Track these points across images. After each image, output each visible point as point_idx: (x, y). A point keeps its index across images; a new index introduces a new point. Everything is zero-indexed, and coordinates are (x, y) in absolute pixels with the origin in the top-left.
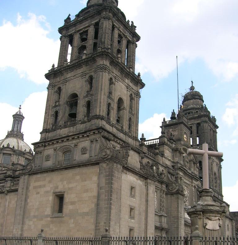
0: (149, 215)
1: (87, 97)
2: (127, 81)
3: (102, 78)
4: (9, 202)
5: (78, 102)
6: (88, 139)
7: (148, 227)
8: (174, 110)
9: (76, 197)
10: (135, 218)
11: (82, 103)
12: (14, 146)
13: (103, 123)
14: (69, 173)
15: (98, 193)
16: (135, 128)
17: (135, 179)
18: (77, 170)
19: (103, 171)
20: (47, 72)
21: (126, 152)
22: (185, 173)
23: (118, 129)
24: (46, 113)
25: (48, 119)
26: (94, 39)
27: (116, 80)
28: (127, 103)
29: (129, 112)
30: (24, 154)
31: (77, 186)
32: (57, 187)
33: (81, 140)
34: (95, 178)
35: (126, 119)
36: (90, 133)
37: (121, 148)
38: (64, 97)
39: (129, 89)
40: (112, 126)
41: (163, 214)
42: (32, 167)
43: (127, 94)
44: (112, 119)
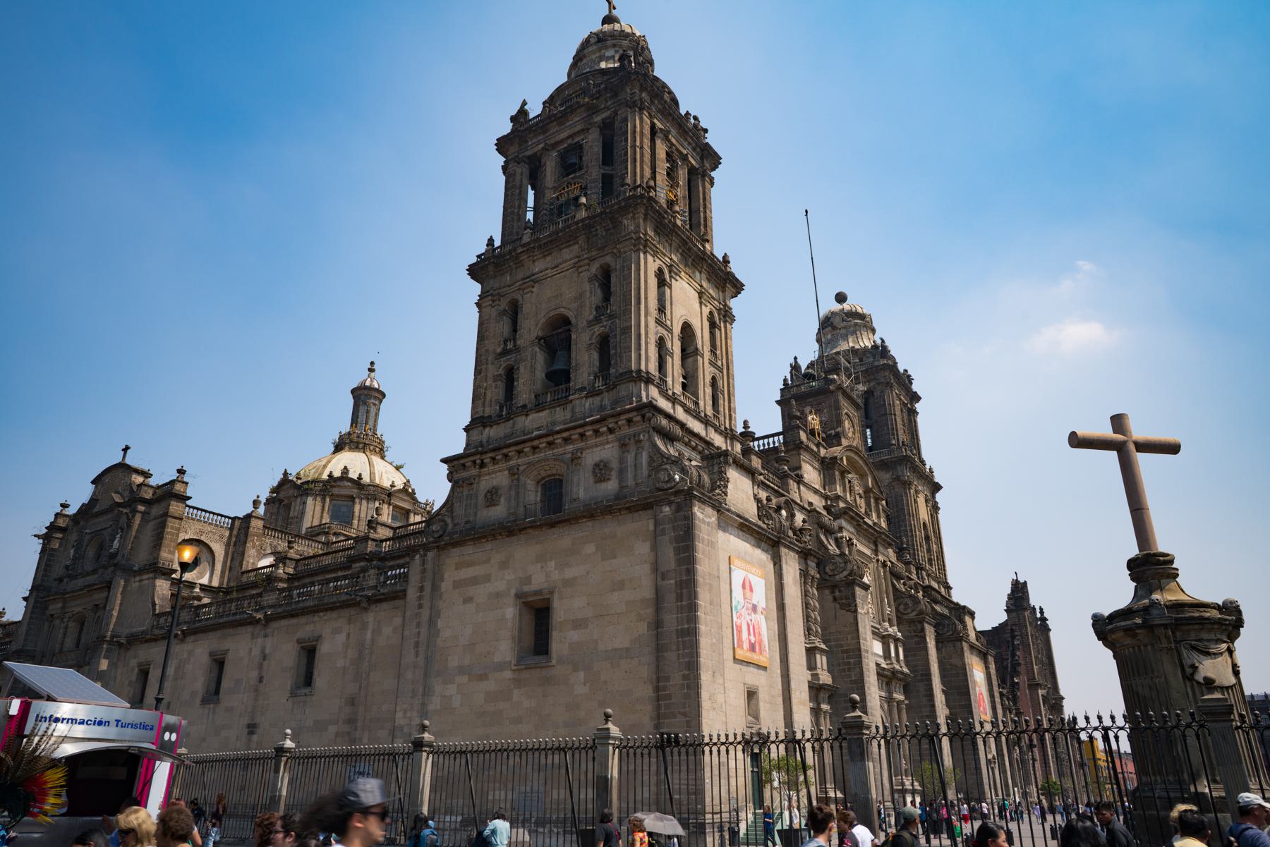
1: (598, 323)
4: (373, 632)
5: (574, 337)
6: (611, 437)
8: (796, 358)
12: (360, 475)
14: (563, 539)
15: (657, 590)
18: (587, 528)
19: (667, 526)
20: (474, 260)
23: (687, 411)
24: (478, 372)
25: (486, 389)
26: (603, 164)
27: (673, 274)
30: (390, 495)
31: (588, 573)
32: (528, 580)
33: (592, 442)
36: (617, 423)
41: (818, 645)
42: (446, 525)
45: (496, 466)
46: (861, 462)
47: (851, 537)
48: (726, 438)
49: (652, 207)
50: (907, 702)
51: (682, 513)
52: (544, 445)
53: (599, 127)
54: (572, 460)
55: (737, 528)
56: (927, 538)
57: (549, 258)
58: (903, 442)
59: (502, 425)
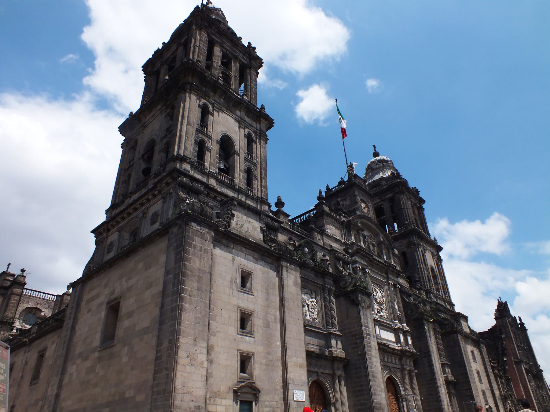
0: (289, 327)
2: (238, 113)
5: (155, 148)
7: (289, 352)
9: (135, 301)
10: (254, 334)
11: (158, 148)
13: (186, 167)
16: (259, 184)
22: (372, 262)
23: (221, 182)
27: (215, 108)
28: (240, 145)
29: (246, 160)
31: (138, 281)
33: (152, 202)
34: (163, 259)
36: (161, 186)
38: (141, 149)
39: (243, 124)
40: (209, 175)
44: (207, 164)
46: (373, 226)
47: (364, 267)
48: (257, 202)
50: (416, 371)
51: (181, 230)
56: (435, 277)
58: (412, 222)
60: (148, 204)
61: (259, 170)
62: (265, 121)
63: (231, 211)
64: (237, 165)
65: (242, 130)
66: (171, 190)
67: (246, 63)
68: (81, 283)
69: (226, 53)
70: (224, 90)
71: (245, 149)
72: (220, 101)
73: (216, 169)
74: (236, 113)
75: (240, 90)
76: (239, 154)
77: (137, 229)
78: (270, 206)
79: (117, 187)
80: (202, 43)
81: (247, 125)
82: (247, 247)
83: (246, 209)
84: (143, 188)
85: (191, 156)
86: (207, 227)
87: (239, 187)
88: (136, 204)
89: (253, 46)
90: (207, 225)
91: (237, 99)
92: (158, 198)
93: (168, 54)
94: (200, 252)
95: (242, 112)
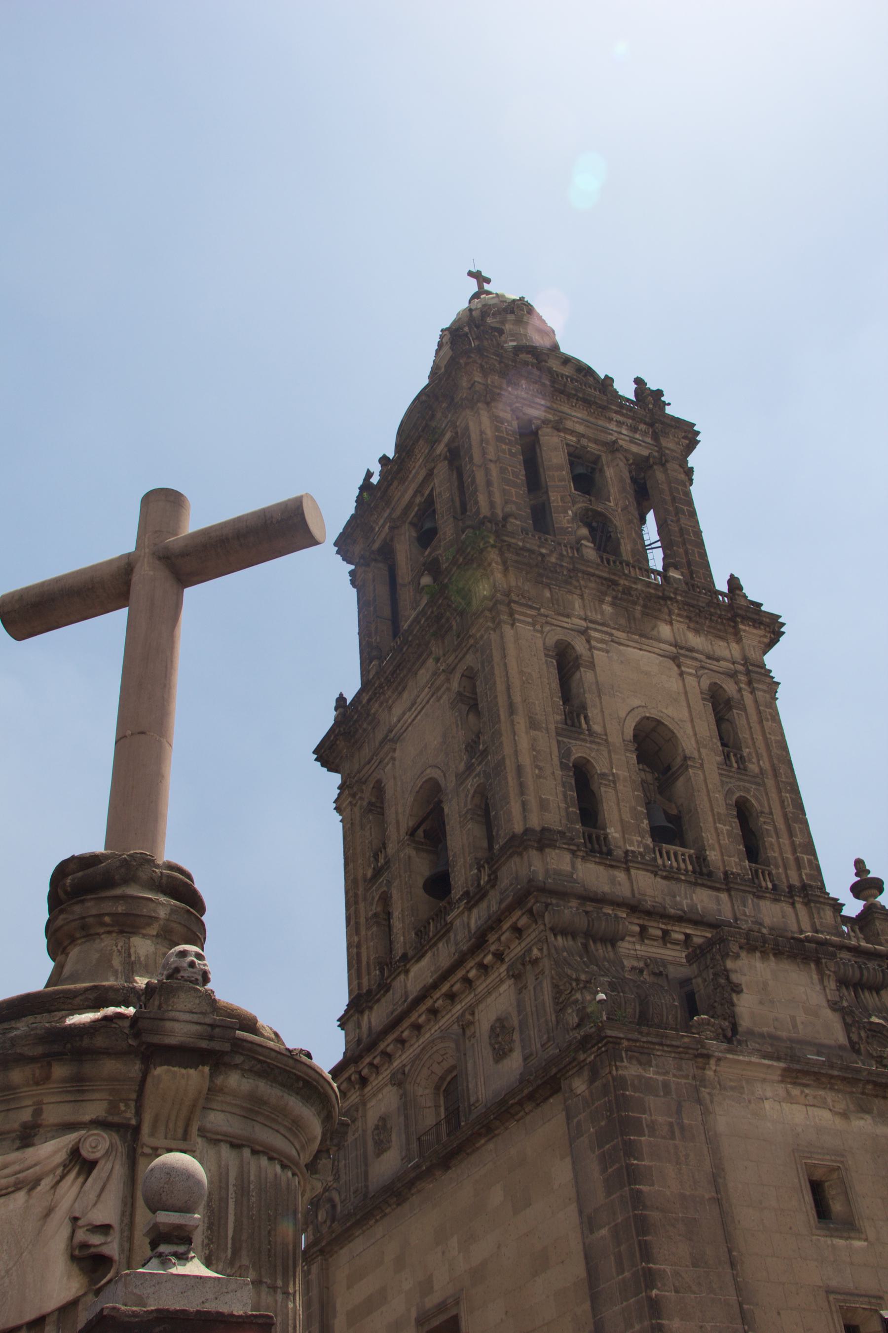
2: (665, 630)
3: (504, 656)
5: (446, 810)
6: (503, 968)
15: (586, 1257)
16: (785, 841)
17: (824, 1116)
19: (582, 1117)
21: (715, 975)
28: (695, 734)
33: (481, 987)
35: (712, 810)
36: (499, 939)
37: (691, 959)
39: (689, 662)
42: (334, 1206)
43: (686, 693)
44: (614, 833)
45: (380, 1078)
49: (509, 545)
51: (598, 1083)
52: (423, 1017)
53: (445, 458)
54: (463, 1029)
55: (782, 1081)
57: (405, 695)
59: (383, 1000)
60: (470, 993)
61: (774, 795)
62: (755, 627)
63: (728, 978)
64: (702, 803)
65: (691, 681)
66: (535, 952)
67: (645, 453)
68: (318, 1256)
69: (578, 446)
70: (606, 579)
71: (714, 740)
72: (602, 613)
73: (643, 838)
74: (659, 632)
75: (647, 543)
76: (702, 765)
77: (454, 1067)
78: (837, 906)
79: (356, 939)
80: (504, 447)
81: (701, 661)
82: (804, 1081)
83: (772, 957)
84: (440, 939)
85: (564, 821)
86: (673, 1055)
87: (726, 873)
88: (431, 997)
89: (652, 385)
90: (669, 1049)
91: (652, 591)
92: (496, 974)
93: (405, 494)
94: (671, 1142)
95: (676, 625)
